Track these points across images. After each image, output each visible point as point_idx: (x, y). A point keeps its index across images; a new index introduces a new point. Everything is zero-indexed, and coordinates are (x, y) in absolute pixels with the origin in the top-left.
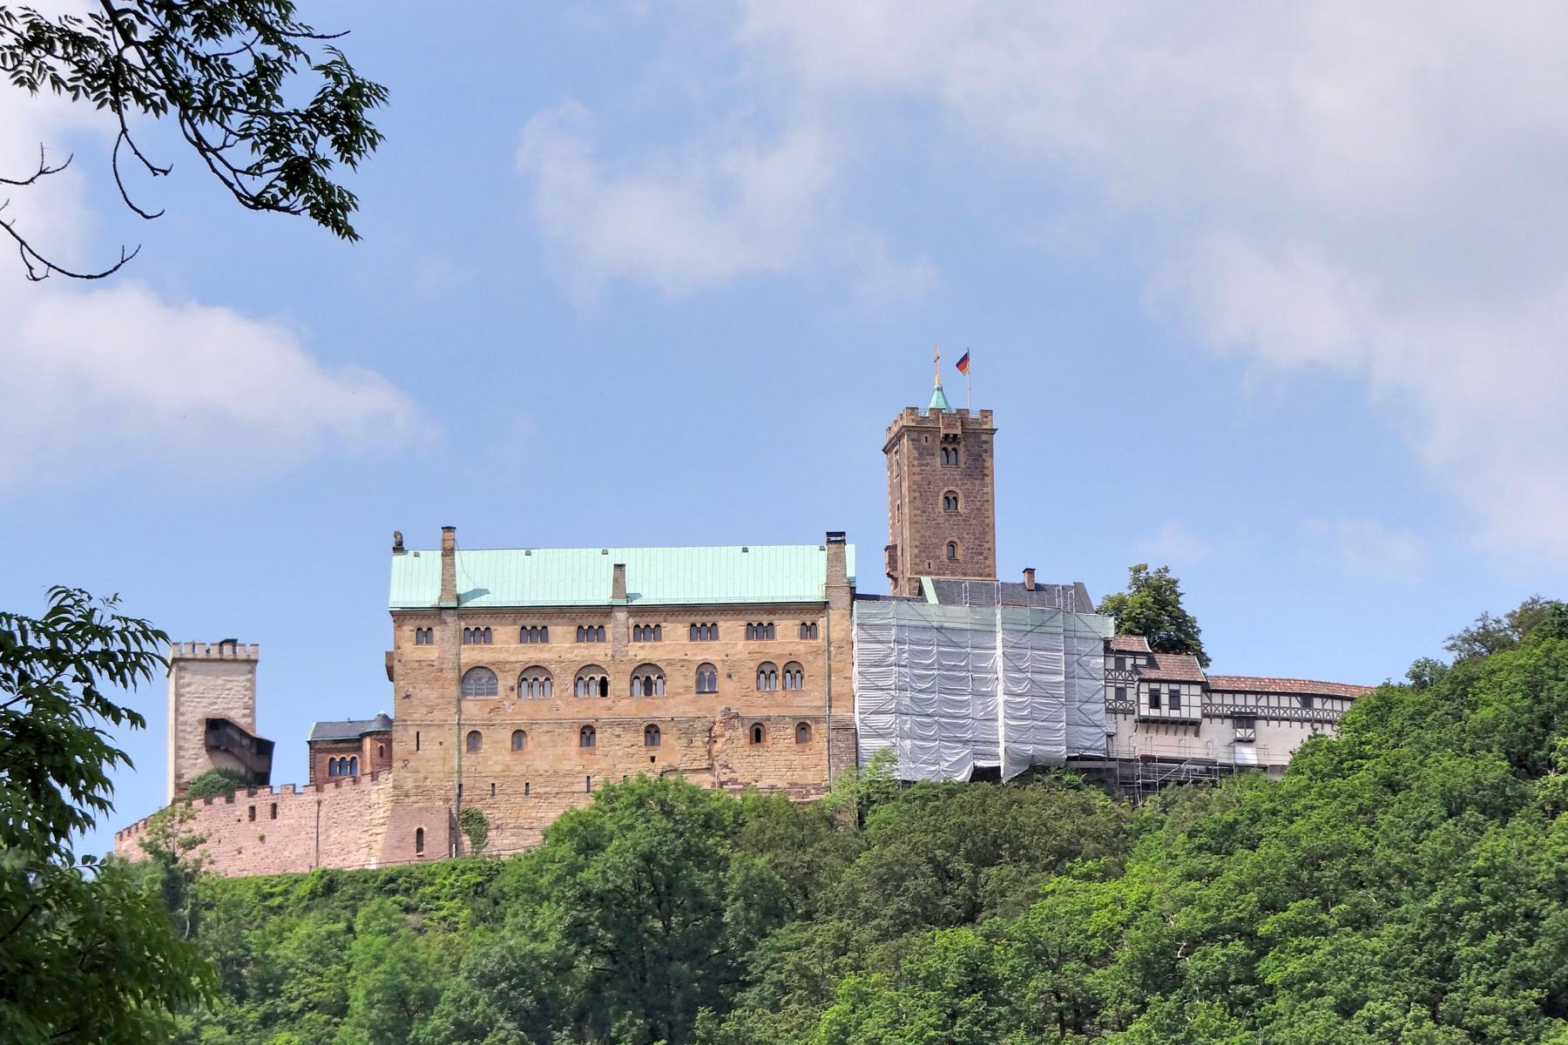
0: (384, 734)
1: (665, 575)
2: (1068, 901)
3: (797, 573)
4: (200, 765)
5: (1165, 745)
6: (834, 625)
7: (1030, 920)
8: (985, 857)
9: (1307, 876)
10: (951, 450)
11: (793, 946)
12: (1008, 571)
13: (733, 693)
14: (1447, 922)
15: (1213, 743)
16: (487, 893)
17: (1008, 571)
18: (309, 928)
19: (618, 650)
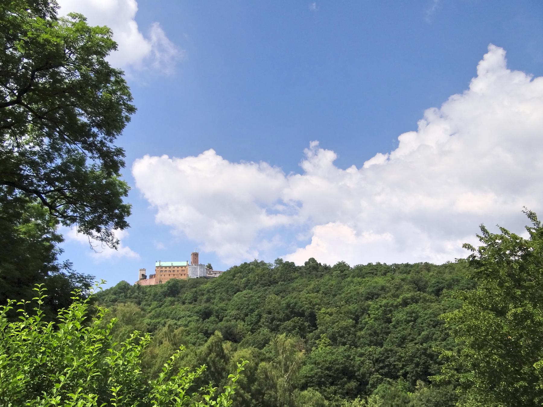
0: (155, 275)
1: (176, 264)
2: (203, 286)
3: (184, 264)
4: (141, 277)
5: (210, 275)
6: (187, 267)
7: (200, 288)
8: (197, 283)
9: (219, 285)
10: (196, 255)
11: (184, 290)
12: (199, 263)
13: (180, 272)
14: (228, 288)
15: (213, 275)
16: (162, 286)
17: (199, 263)
18: (149, 289)
19: (172, 269)
